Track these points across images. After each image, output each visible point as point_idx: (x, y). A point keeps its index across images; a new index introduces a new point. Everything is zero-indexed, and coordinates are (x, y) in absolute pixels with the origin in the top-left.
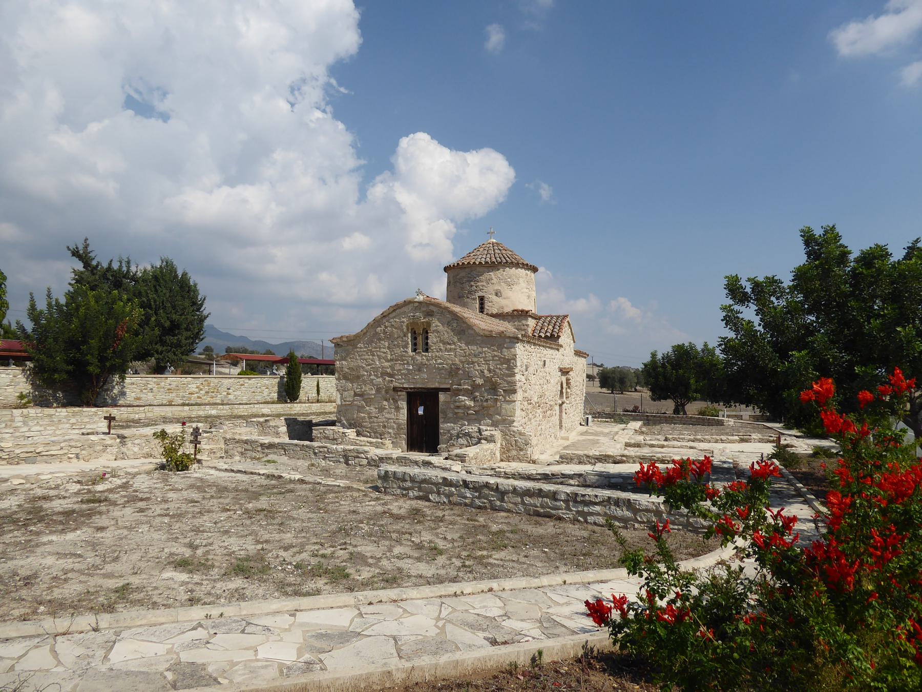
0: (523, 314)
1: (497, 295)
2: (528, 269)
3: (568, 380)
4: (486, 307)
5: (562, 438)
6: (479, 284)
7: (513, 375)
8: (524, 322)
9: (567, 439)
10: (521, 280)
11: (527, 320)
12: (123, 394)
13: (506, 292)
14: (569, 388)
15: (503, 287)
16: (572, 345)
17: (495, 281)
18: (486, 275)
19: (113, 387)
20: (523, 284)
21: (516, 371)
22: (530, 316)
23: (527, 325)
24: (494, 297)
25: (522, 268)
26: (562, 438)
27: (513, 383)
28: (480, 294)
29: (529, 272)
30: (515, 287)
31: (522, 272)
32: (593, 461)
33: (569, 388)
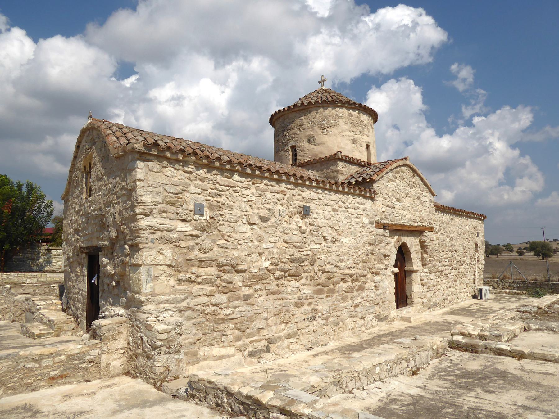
0: (335, 158)
1: (309, 141)
2: (354, 109)
3: (422, 243)
4: (298, 157)
5: (403, 319)
6: (291, 132)
7: (133, 218)
8: (333, 168)
9: (408, 320)
10: (341, 122)
11: (336, 164)
12: (49, 262)
13: (321, 136)
14: (426, 252)
15: (317, 133)
16: (426, 197)
17: (307, 125)
18: (298, 121)
19: (40, 257)
20: (343, 125)
21: (138, 210)
22: (341, 160)
23: (337, 171)
24: (306, 145)
25: (342, 107)
26: (403, 319)
27: (135, 233)
28: (292, 143)
29: (356, 113)
30: (333, 130)
31: (344, 112)
32: (236, 407)
33: (426, 252)
